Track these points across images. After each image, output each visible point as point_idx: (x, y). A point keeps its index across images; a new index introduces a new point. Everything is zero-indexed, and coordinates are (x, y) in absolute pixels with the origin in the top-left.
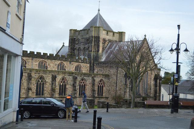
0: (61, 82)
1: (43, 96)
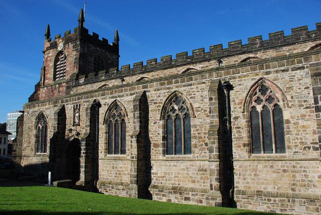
0: (258, 101)
1: (190, 156)
